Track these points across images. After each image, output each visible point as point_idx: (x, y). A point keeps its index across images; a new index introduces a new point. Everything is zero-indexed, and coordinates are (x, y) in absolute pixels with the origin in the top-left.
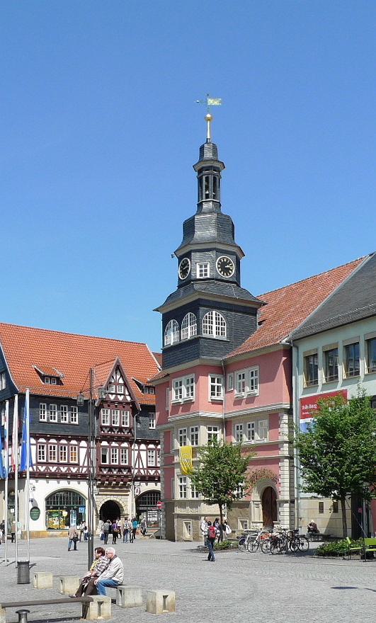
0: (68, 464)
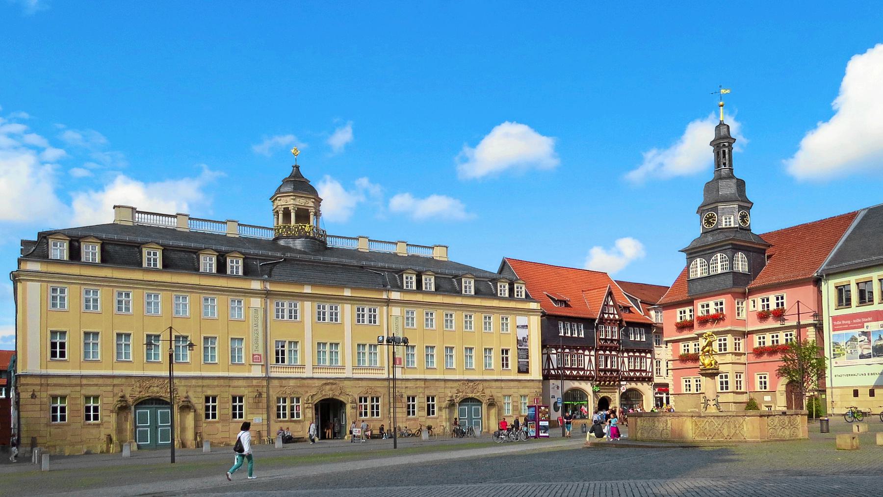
0: (578, 369)
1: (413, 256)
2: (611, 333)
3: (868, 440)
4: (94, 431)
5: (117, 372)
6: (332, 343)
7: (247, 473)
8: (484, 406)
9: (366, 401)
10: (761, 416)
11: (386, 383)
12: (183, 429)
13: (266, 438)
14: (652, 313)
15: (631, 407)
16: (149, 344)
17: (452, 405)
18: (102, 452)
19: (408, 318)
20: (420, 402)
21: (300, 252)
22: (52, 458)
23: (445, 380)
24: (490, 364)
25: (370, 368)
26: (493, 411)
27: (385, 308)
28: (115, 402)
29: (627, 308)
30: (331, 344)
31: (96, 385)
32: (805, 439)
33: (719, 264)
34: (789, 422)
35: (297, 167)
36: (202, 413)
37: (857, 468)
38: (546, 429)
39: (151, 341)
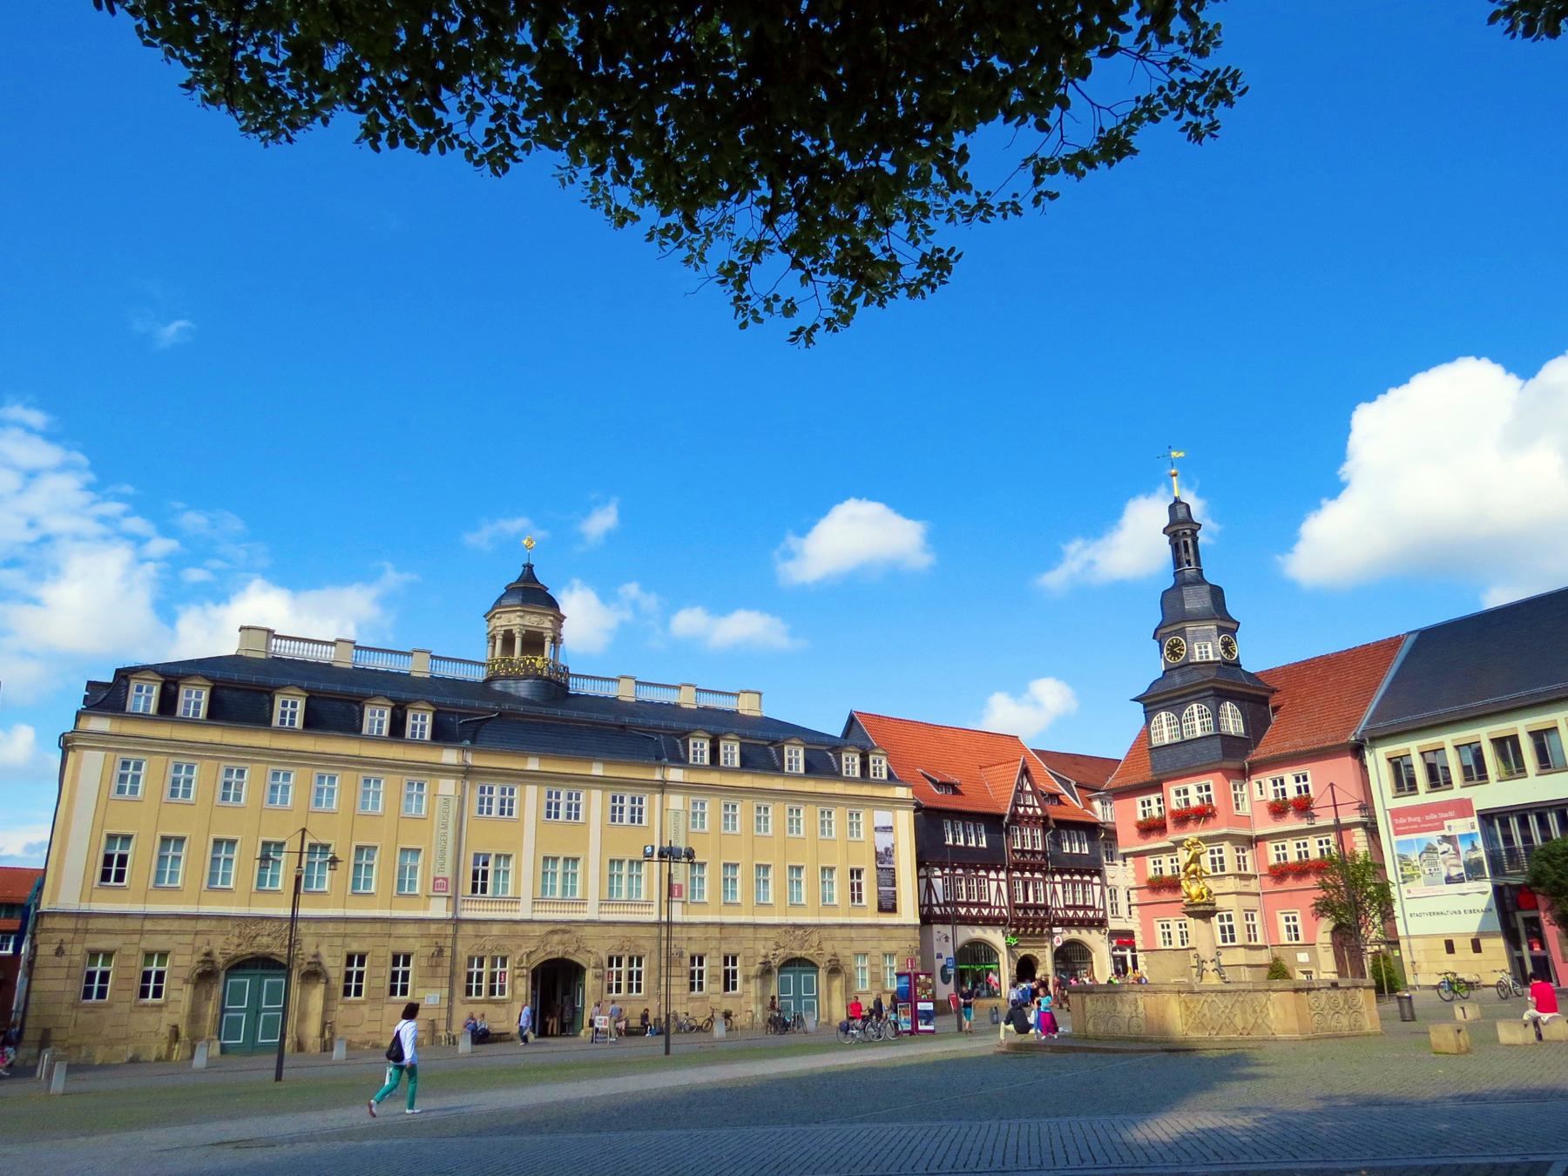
0: (979, 905)
1: (705, 709)
2: (1030, 840)
3: (1483, 1034)
4: (151, 1018)
5: (205, 909)
6: (568, 858)
7: (406, 1103)
8: (822, 974)
9: (619, 964)
10: (1296, 991)
11: (655, 931)
12: (303, 1017)
13: (443, 1034)
14: (1097, 804)
15: (1074, 975)
16: (265, 858)
17: (766, 972)
18: (158, 1059)
19: (695, 814)
20: (712, 966)
21: (525, 701)
22: (72, 1069)
23: (755, 926)
24: (831, 896)
25: (629, 903)
26: (838, 983)
27: (658, 797)
28: (194, 964)
29: (1054, 797)
30: (566, 860)
31: (167, 932)
32: (1376, 1034)
33: (1197, 722)
34: (1346, 1001)
35: (529, 567)
36: (339, 984)
37: (1474, 1089)
38: (928, 1016)
39: (268, 854)
